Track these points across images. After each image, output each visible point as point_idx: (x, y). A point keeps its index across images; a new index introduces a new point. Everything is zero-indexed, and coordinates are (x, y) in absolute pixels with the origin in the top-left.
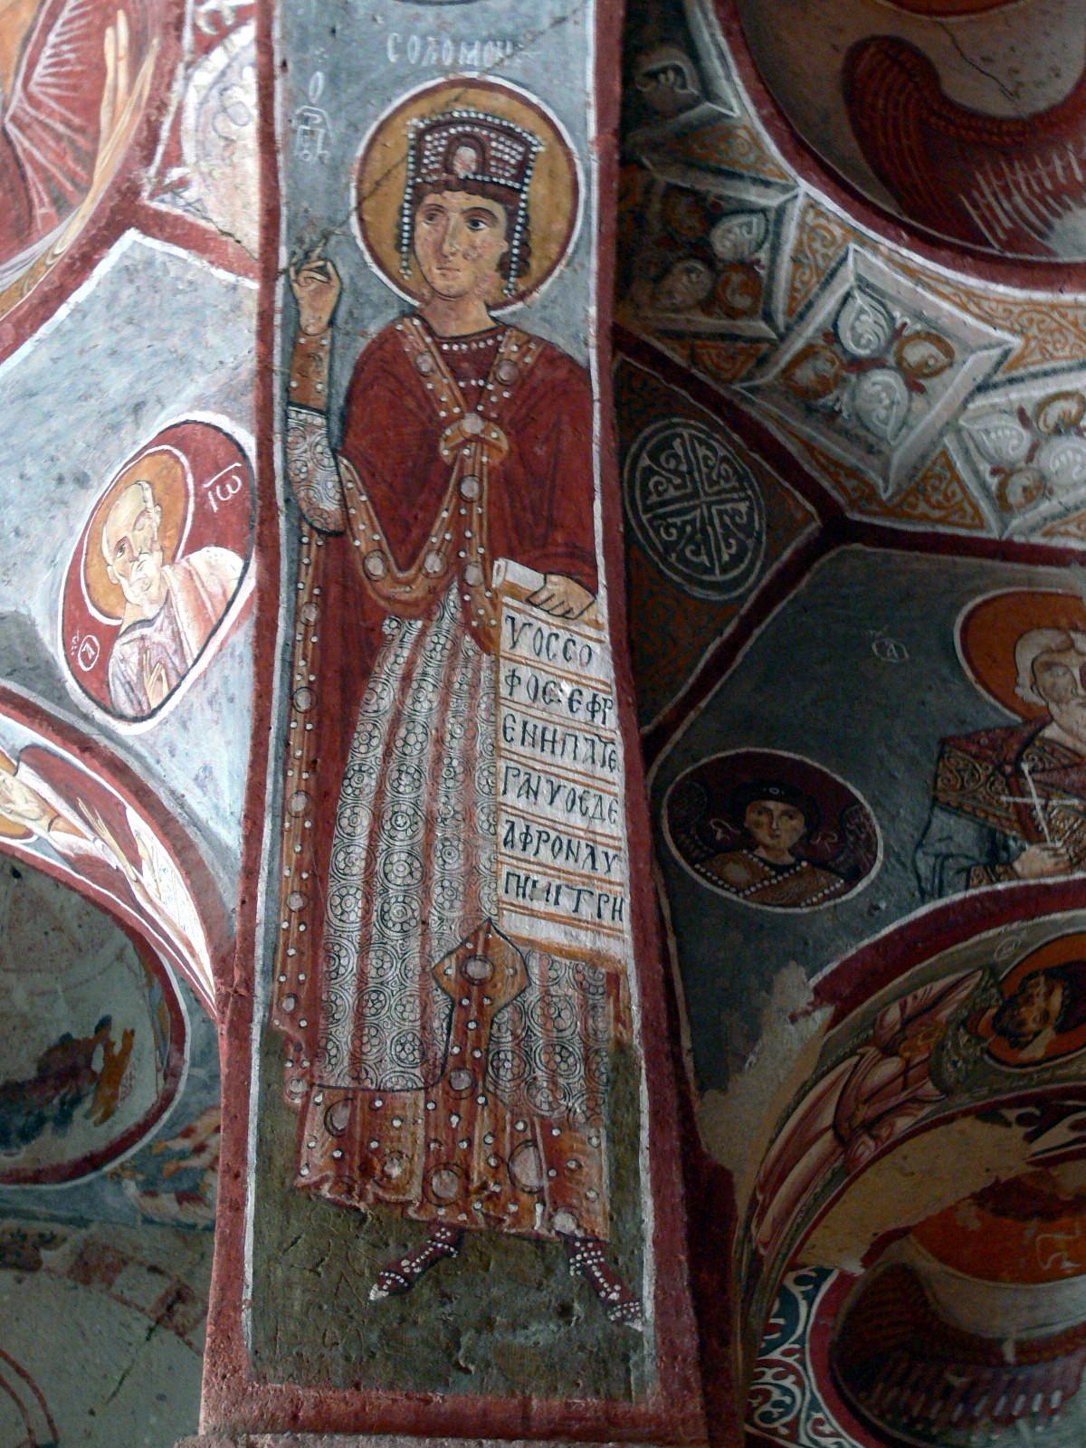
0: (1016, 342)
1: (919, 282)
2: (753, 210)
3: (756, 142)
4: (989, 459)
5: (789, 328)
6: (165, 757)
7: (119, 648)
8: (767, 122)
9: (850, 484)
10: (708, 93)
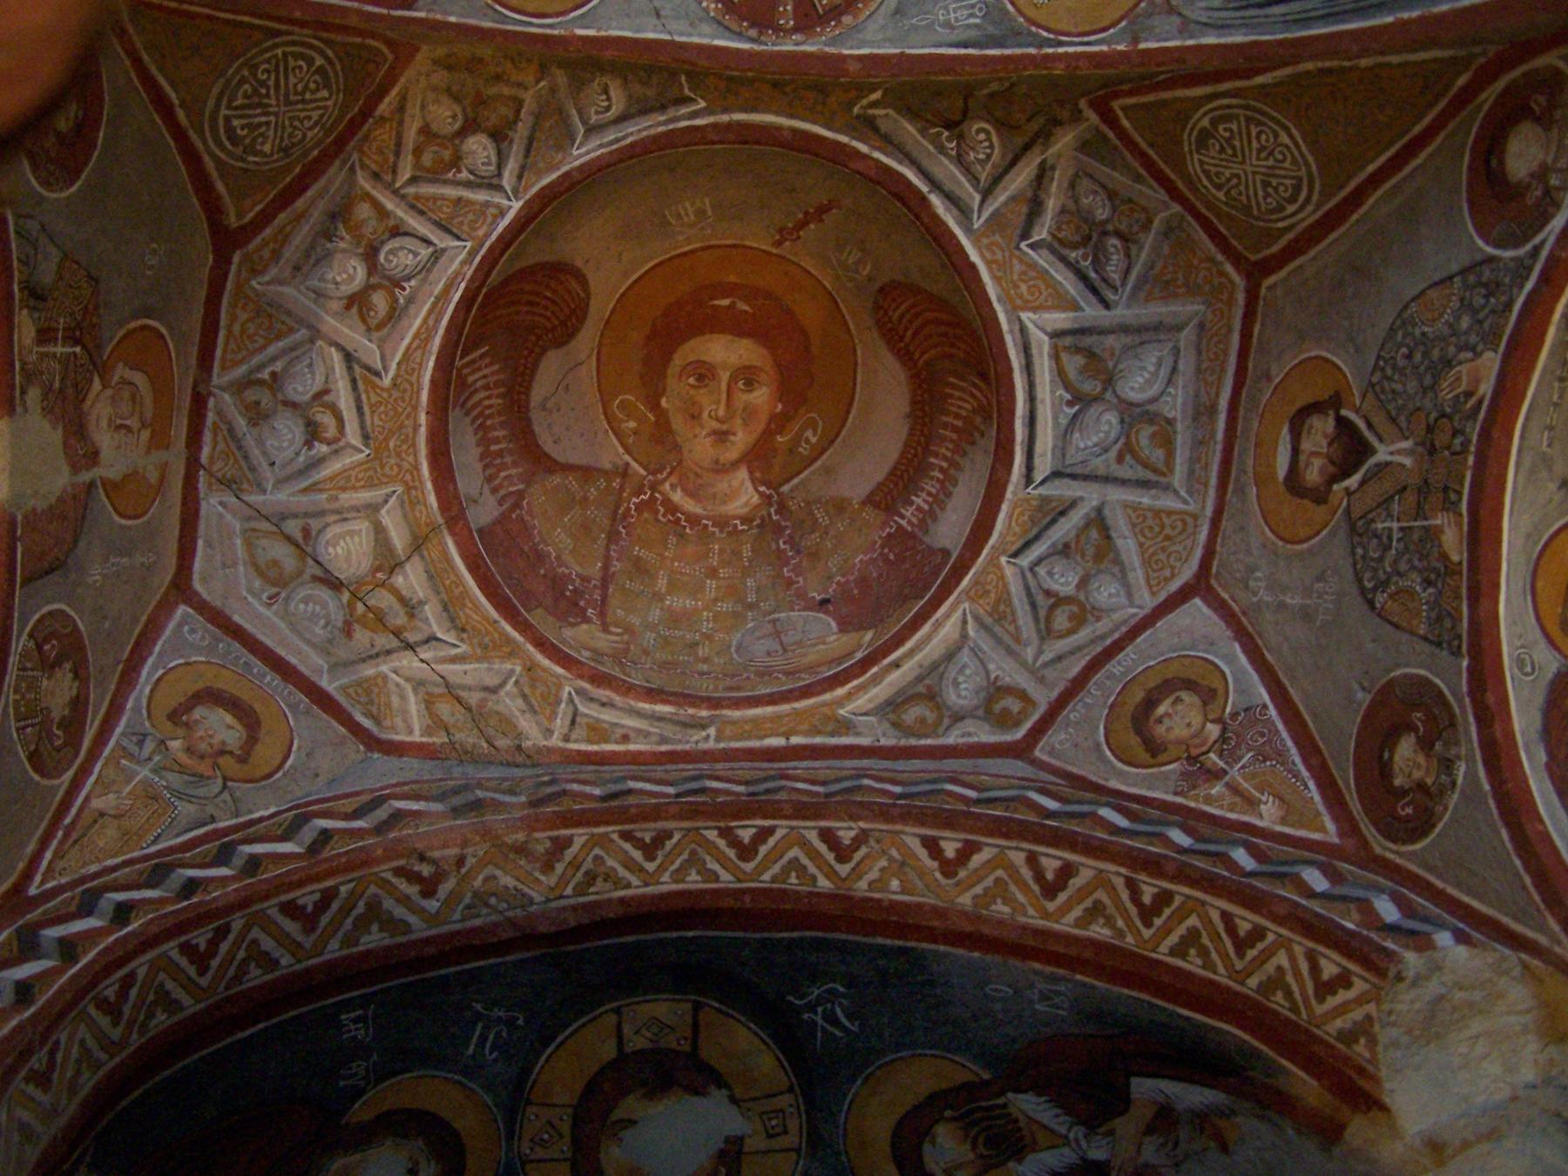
0: (387, 382)
1: (438, 299)
2: (500, 167)
3: (552, 168)
4: (285, 369)
5: (403, 197)
8: (567, 175)
9: (266, 254)
10: (591, 130)
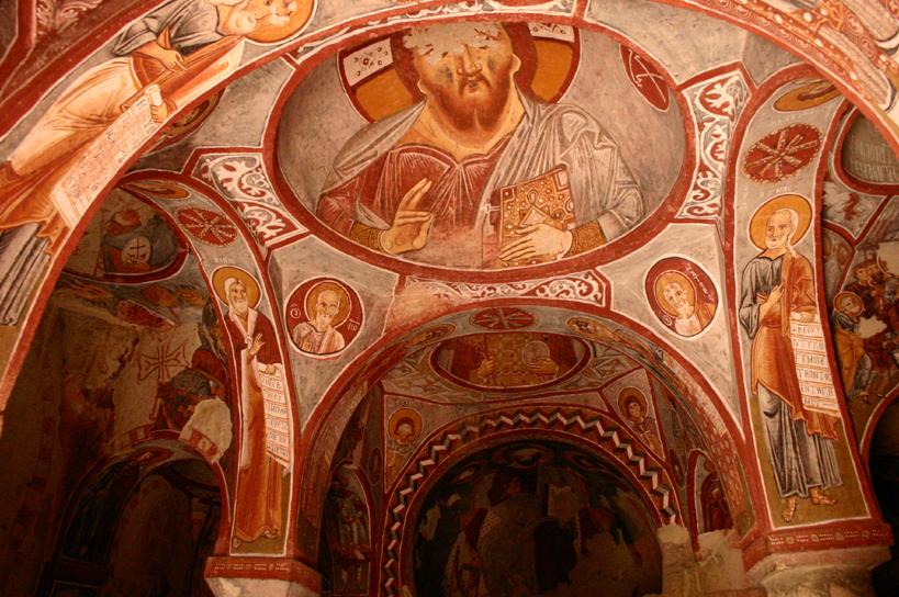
6: (296, 362)
7: (304, 324)
